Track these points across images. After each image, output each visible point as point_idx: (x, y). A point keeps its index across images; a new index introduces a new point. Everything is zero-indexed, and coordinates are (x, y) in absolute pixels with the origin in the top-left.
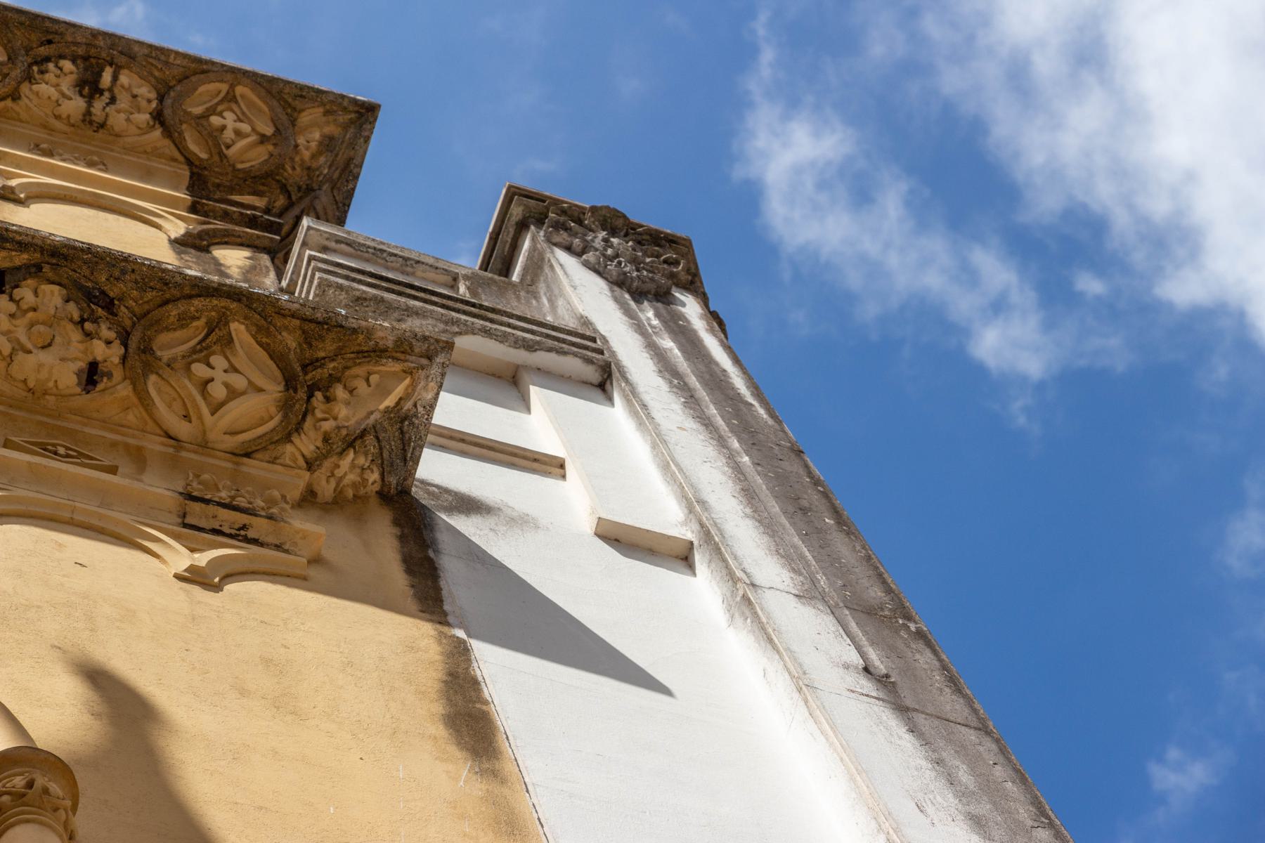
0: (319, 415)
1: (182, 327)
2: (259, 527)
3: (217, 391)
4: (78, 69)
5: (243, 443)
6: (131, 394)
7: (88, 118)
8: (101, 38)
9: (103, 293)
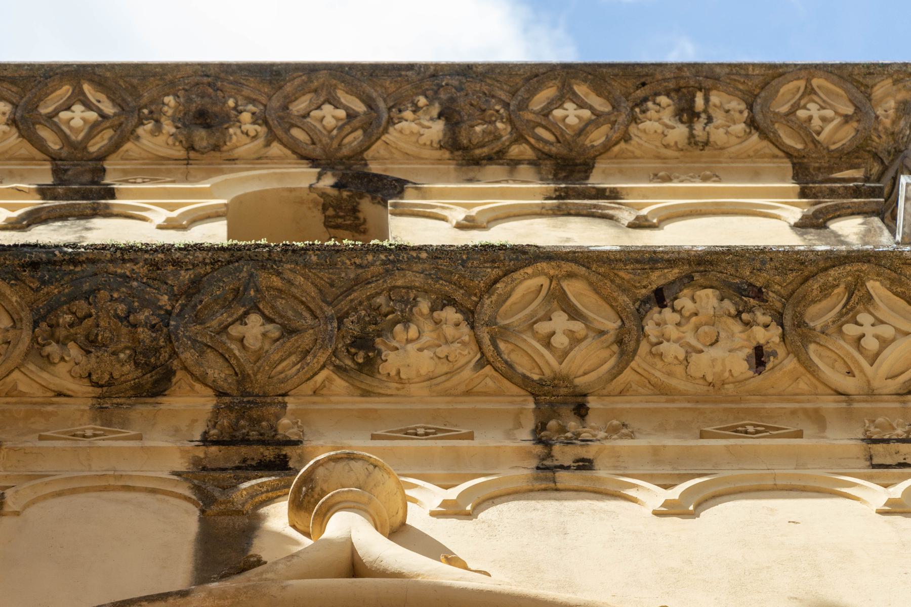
1: (826, 296)
3: (871, 344)
4: (673, 101)
5: (905, 383)
6: (798, 365)
7: (692, 140)
8: (685, 69)
9: (750, 285)
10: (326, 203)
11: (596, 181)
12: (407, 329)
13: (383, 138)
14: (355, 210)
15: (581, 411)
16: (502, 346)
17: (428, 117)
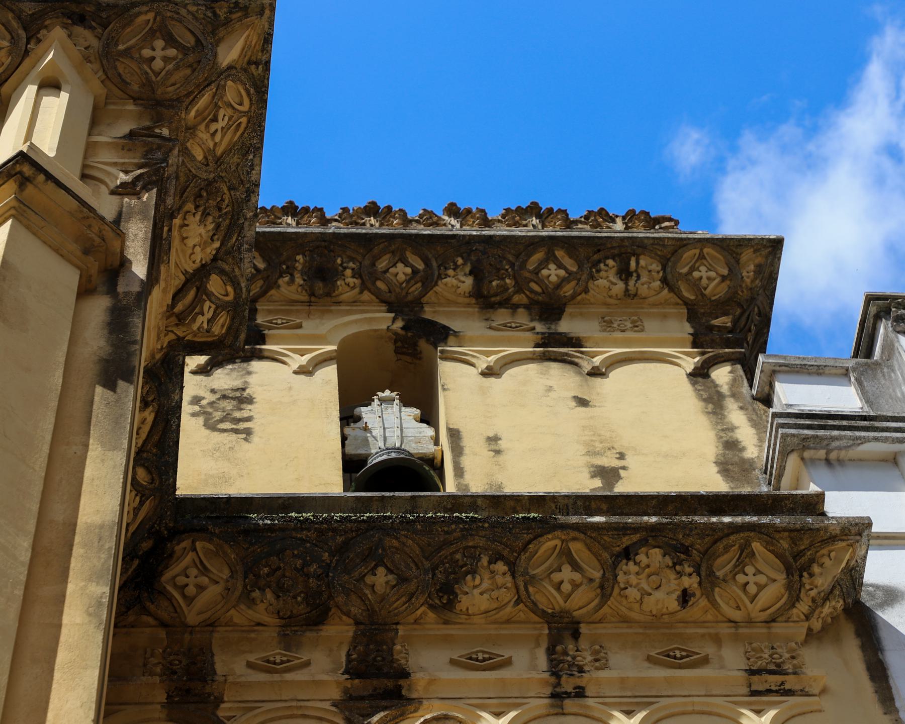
0: (808, 587)
1: (727, 552)
2: (791, 682)
3: (752, 589)
4: (617, 263)
5: (770, 615)
6: (707, 603)
7: (627, 294)
8: (626, 241)
9: (682, 544)
10: (397, 339)
11: (565, 326)
12: (474, 579)
13: (434, 289)
14: (415, 345)
15: (576, 635)
16: (531, 589)
17: (463, 273)
